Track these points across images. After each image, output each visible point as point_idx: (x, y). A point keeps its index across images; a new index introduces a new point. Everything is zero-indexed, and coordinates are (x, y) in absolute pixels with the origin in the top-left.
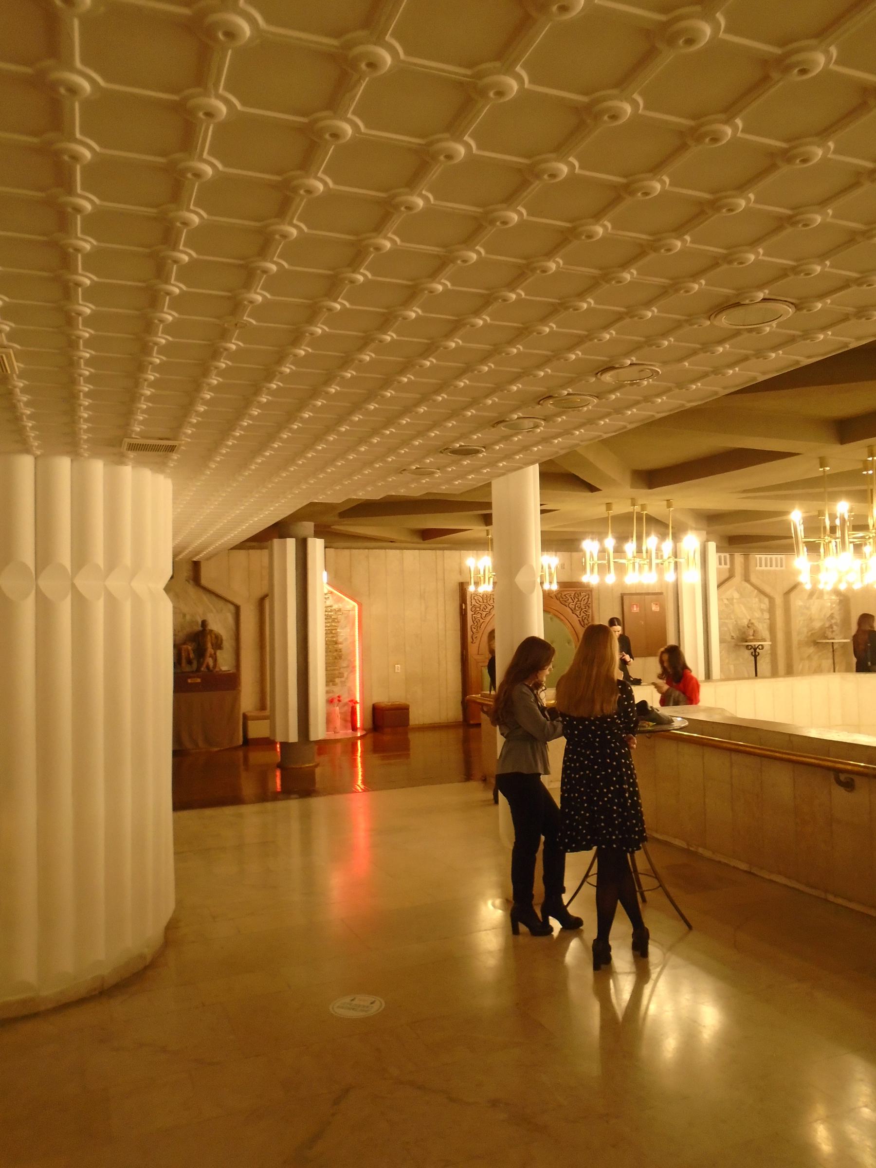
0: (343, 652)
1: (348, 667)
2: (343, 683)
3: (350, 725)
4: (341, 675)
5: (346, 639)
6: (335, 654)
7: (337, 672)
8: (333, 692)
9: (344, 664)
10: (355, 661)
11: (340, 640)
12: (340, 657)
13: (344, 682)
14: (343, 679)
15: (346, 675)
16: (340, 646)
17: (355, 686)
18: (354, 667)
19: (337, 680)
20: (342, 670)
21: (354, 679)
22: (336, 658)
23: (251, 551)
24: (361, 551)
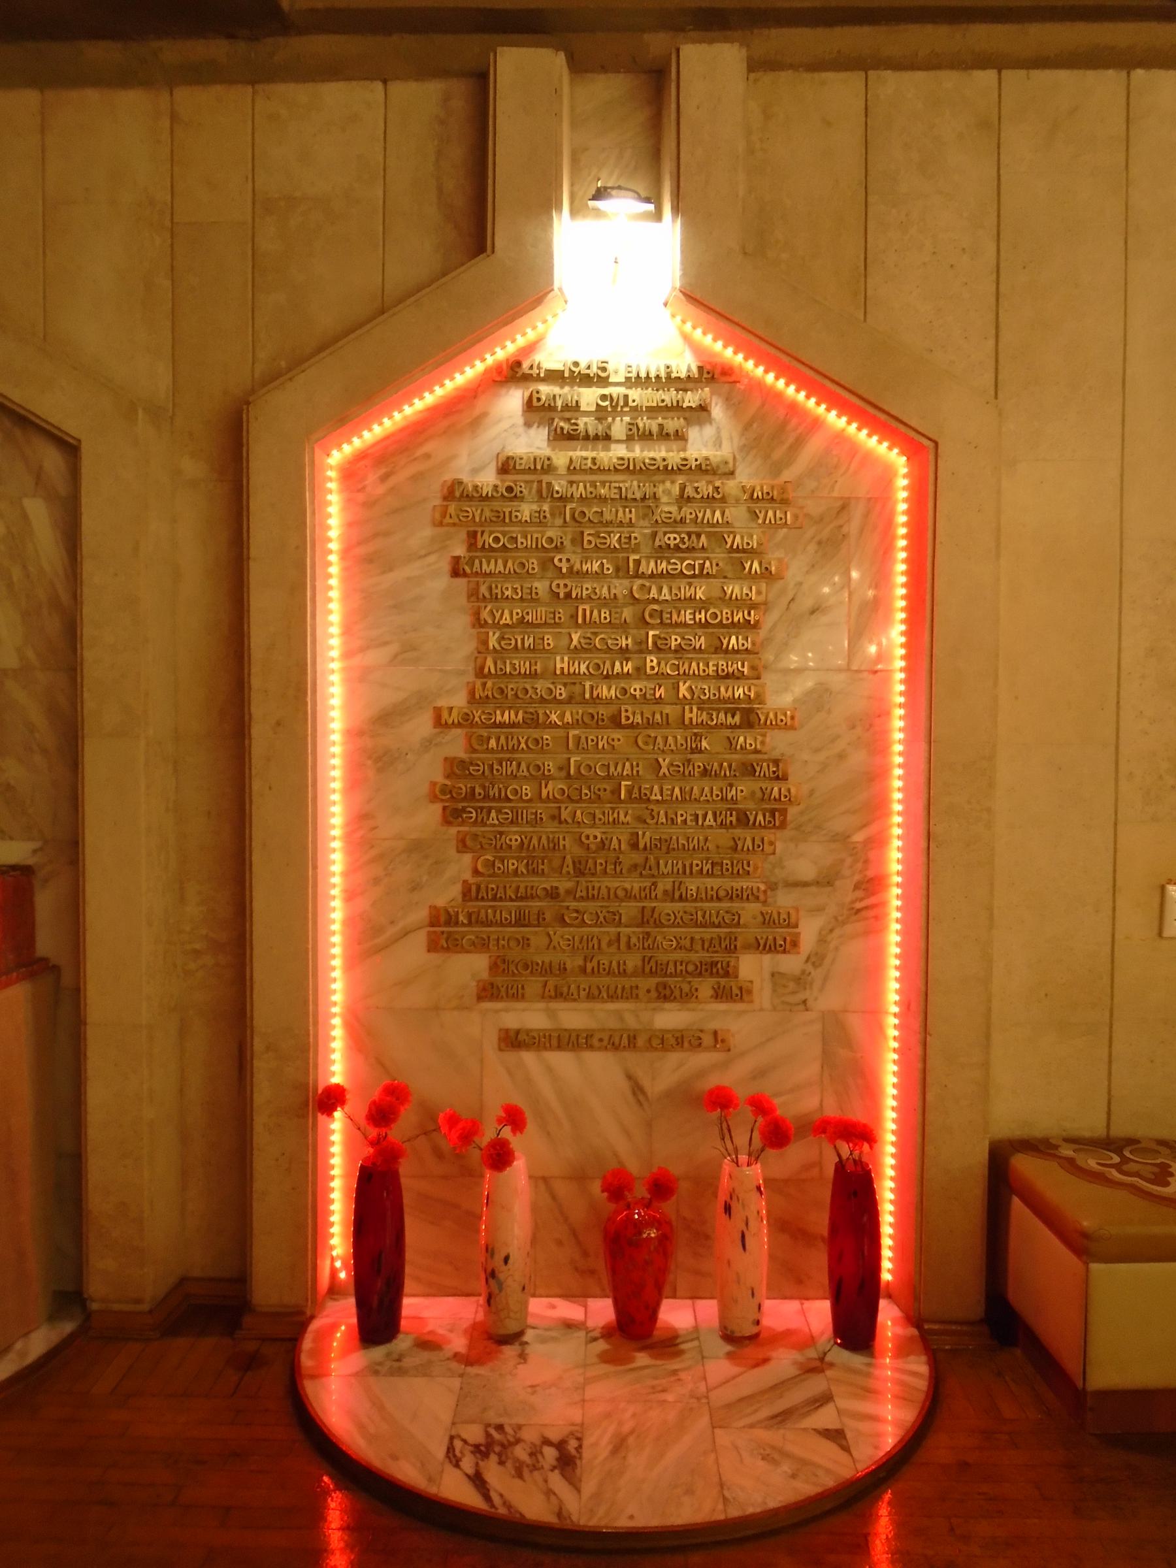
0: (798, 783)
1: (826, 881)
2: (792, 990)
3: (818, 1262)
4: (777, 938)
5: (820, 698)
6: (743, 788)
7: (749, 911)
8: (719, 1040)
9: (802, 859)
10: (879, 842)
11: (781, 698)
12: (777, 816)
13: (801, 981)
14: (790, 963)
15: (809, 931)
16: (777, 743)
17: (874, 1013)
18: (874, 884)
19: (751, 967)
20: (784, 900)
21: (874, 972)
22: (744, 820)
23: (188, 98)
24: (949, 80)
